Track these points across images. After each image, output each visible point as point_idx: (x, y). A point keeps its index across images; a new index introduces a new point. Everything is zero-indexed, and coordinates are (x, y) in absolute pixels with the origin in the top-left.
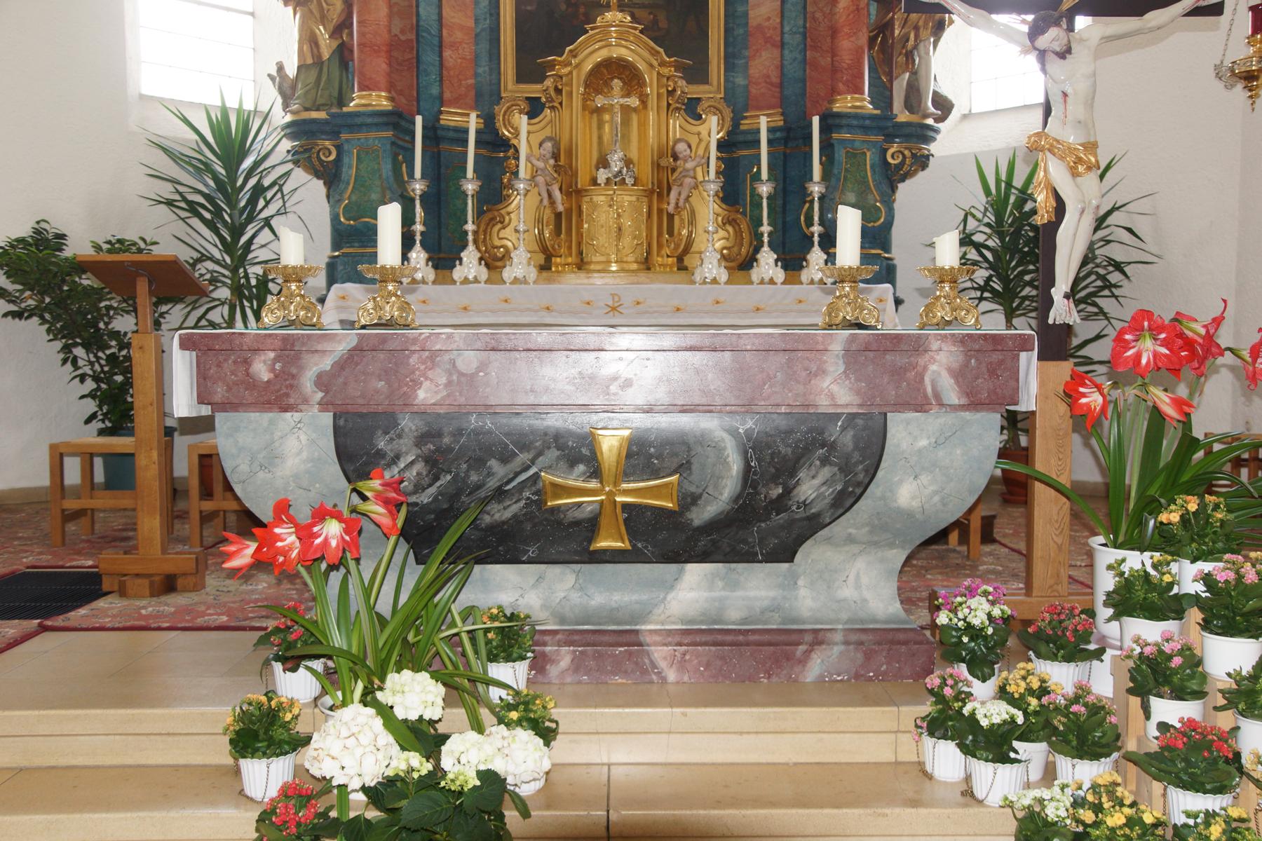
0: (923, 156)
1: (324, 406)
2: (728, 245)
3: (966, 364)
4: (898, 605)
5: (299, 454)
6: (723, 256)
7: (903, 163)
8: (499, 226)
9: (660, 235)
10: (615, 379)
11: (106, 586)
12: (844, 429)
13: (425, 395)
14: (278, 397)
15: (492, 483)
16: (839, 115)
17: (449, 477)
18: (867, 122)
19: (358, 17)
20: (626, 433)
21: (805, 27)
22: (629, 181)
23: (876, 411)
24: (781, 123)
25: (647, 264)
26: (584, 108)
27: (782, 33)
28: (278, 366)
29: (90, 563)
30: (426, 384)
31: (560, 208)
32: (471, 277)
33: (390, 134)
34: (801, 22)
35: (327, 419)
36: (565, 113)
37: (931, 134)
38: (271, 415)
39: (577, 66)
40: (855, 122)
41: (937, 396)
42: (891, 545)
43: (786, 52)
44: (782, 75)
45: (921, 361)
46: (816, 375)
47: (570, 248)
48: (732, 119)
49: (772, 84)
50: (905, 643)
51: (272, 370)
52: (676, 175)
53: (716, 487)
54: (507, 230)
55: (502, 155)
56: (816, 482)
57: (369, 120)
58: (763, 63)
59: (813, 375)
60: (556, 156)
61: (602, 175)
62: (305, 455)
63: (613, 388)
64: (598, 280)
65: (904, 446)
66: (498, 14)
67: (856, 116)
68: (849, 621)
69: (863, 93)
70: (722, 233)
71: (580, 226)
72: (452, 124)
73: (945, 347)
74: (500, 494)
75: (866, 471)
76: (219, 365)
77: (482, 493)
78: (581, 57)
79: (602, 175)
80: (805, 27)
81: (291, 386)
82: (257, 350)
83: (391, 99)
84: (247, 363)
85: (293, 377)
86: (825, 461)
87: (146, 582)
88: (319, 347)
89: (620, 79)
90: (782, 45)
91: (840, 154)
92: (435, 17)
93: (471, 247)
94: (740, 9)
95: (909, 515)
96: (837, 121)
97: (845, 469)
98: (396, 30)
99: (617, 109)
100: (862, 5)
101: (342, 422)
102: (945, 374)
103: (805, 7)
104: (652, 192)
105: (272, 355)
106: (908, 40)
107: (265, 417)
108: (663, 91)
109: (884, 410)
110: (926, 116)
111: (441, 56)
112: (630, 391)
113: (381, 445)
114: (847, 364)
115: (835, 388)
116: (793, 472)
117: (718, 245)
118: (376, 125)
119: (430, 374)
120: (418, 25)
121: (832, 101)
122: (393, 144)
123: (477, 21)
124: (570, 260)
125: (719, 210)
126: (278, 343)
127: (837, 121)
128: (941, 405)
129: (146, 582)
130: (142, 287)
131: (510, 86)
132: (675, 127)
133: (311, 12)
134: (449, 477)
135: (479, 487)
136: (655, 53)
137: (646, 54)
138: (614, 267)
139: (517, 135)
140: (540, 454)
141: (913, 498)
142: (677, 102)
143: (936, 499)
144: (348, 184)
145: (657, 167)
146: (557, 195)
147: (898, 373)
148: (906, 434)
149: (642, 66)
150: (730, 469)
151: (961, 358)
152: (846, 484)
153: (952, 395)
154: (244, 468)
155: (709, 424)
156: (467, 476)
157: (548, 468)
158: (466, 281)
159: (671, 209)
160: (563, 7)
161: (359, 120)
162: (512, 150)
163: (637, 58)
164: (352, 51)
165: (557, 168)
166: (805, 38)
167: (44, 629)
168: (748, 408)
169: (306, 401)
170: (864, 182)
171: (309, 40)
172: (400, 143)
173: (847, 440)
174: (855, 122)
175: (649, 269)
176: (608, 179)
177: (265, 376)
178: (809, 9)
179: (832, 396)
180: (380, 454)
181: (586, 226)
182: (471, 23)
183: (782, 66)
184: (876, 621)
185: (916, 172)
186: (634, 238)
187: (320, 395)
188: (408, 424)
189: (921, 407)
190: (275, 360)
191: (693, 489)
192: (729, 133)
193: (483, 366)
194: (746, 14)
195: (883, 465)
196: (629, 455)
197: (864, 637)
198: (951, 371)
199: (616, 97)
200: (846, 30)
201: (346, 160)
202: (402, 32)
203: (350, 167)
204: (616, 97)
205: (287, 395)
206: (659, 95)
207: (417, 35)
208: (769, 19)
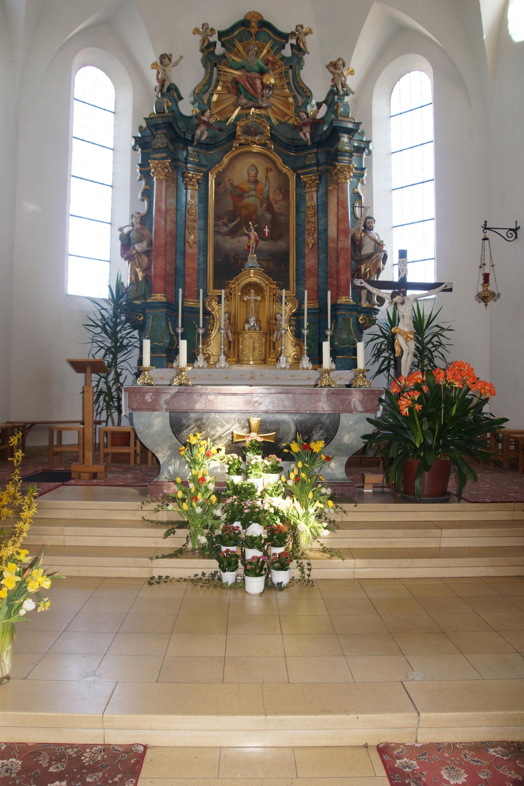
0: (373, 320)
1: (167, 410)
2: (297, 354)
3: (364, 398)
4: (345, 475)
5: (158, 424)
6: (294, 358)
7: (365, 323)
8: (206, 345)
9: (270, 350)
10: (256, 402)
11: (73, 475)
12: (327, 418)
13: (198, 406)
14: (153, 407)
15: (218, 434)
16: (339, 305)
17: (205, 432)
18: (351, 307)
19: (154, 265)
20: (259, 419)
21: (327, 269)
22: (258, 329)
23: (336, 412)
24: (318, 306)
25: (264, 361)
26: (241, 300)
27: (318, 271)
28: (153, 397)
29: (63, 469)
30: (199, 403)
31: (231, 339)
32: (201, 366)
33: (165, 310)
34: (325, 268)
35: (167, 414)
36: (233, 302)
37: (376, 311)
38: (150, 412)
39: (238, 284)
40: (346, 307)
41: (355, 408)
42: (342, 456)
43: (320, 279)
44: (318, 287)
45: (350, 397)
46: (318, 401)
47: (234, 354)
48: (299, 305)
49: (314, 291)
50: (347, 486)
51: (152, 398)
52: (276, 326)
53: (287, 436)
54: (209, 347)
55: (207, 317)
56: (318, 435)
57: (157, 305)
58: (311, 282)
59: (317, 401)
60: (229, 319)
61: (247, 326)
62: (160, 425)
63: (256, 405)
64: (245, 368)
65: (345, 423)
66: (207, 263)
67: (346, 305)
68: (329, 480)
69: (349, 296)
70: (295, 349)
71: (238, 346)
72: (188, 305)
73: (357, 393)
74: (220, 437)
75: (334, 431)
76: (135, 397)
77: (214, 438)
78: (240, 281)
79: (247, 326)
80: (327, 269)
81: (157, 403)
82: (146, 392)
83: (165, 297)
84: (144, 396)
85: (158, 400)
86: (321, 428)
87: (88, 474)
88: (166, 391)
89: (254, 290)
90: (318, 276)
91: (340, 319)
92: (182, 264)
93: (201, 355)
94: (302, 262)
95: (347, 445)
96: (339, 307)
97: (327, 431)
98: (167, 270)
99: (253, 301)
100: (348, 262)
101: (172, 415)
102: (357, 402)
103: (327, 262)
104: (267, 333)
105: (151, 394)
106: (367, 275)
107: (149, 413)
108: (272, 294)
109: (339, 412)
110: (375, 305)
111: (184, 279)
112: (261, 406)
113: (184, 422)
114: (327, 398)
115: (324, 405)
116: (311, 431)
117: (293, 354)
118: (160, 307)
119: (200, 400)
120: (176, 268)
121: (337, 299)
122: (166, 314)
123: (198, 265)
124: (234, 359)
125: (293, 340)
126: (154, 391)
127: (339, 307)
128: (356, 411)
129: (88, 474)
130: (89, 370)
131: (211, 290)
132: (276, 308)
133: (135, 263)
134: (205, 432)
135: (214, 435)
136: (268, 280)
137: (264, 280)
138: (252, 363)
139: (214, 310)
140: (233, 425)
141: (348, 440)
142: (277, 298)
143: (356, 440)
144: (148, 329)
145: (269, 323)
146: (230, 334)
147: (343, 401)
148: (346, 420)
149: (263, 284)
150: (291, 430)
151: (362, 397)
152: (328, 435)
153: (360, 409)
154: (141, 429)
155: (286, 417)
156: (210, 432)
157: (236, 430)
158: (199, 367)
159: (274, 340)
160: (232, 260)
161: (153, 305)
162: (212, 316)
163: (261, 282)
164: (150, 278)
165: (230, 323)
166: (327, 274)
167: (63, 485)
168: (297, 413)
169: (161, 408)
170: (350, 330)
171: (134, 273)
172: (169, 313)
173: (328, 421)
174: (346, 307)
175: (265, 363)
176: (249, 328)
177: (149, 400)
178: (329, 262)
179: (323, 408)
180: (184, 425)
181: (241, 346)
182: (196, 266)
183: (318, 284)
184: (337, 480)
185: (370, 326)
186: (260, 351)
187: (166, 406)
188: (192, 415)
189: (351, 411)
190: (153, 395)
191: (280, 437)
192: (297, 310)
193: (215, 399)
194: (304, 264)
195: (339, 429)
196: (260, 426)
197: (334, 485)
198: (359, 400)
199: (252, 296)
200: (342, 272)
201: (148, 320)
202: (170, 270)
203: (149, 323)
204: (252, 296)
205: (156, 406)
206: (270, 296)
207: (176, 272)
208: (313, 266)
